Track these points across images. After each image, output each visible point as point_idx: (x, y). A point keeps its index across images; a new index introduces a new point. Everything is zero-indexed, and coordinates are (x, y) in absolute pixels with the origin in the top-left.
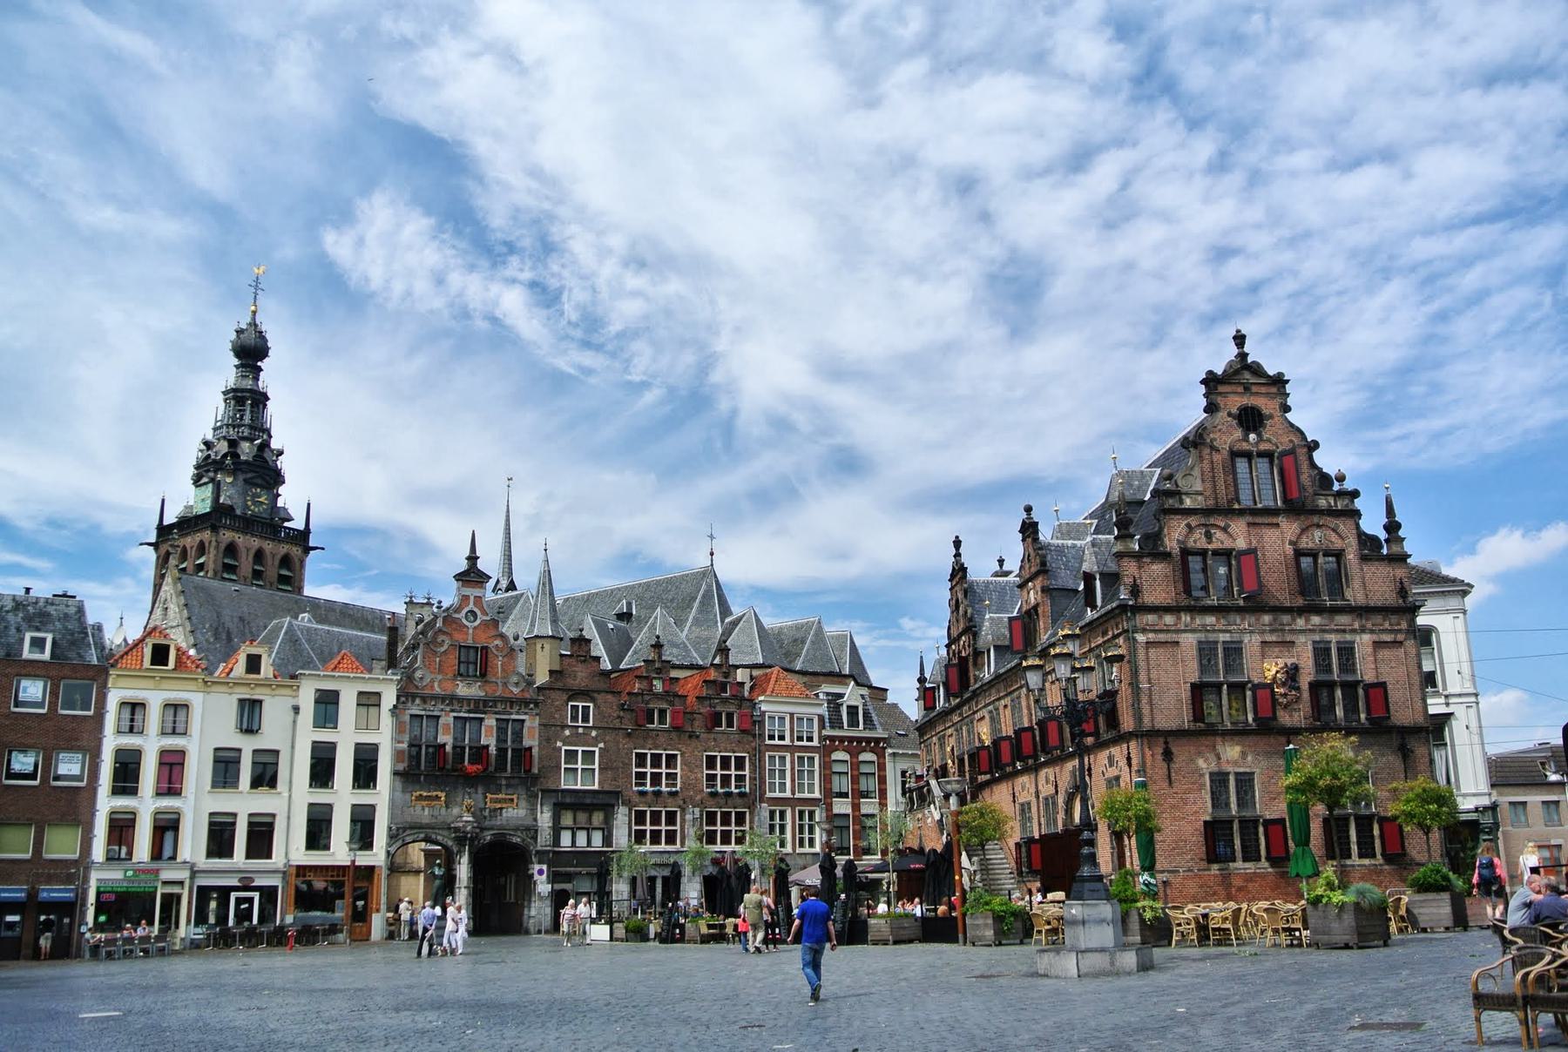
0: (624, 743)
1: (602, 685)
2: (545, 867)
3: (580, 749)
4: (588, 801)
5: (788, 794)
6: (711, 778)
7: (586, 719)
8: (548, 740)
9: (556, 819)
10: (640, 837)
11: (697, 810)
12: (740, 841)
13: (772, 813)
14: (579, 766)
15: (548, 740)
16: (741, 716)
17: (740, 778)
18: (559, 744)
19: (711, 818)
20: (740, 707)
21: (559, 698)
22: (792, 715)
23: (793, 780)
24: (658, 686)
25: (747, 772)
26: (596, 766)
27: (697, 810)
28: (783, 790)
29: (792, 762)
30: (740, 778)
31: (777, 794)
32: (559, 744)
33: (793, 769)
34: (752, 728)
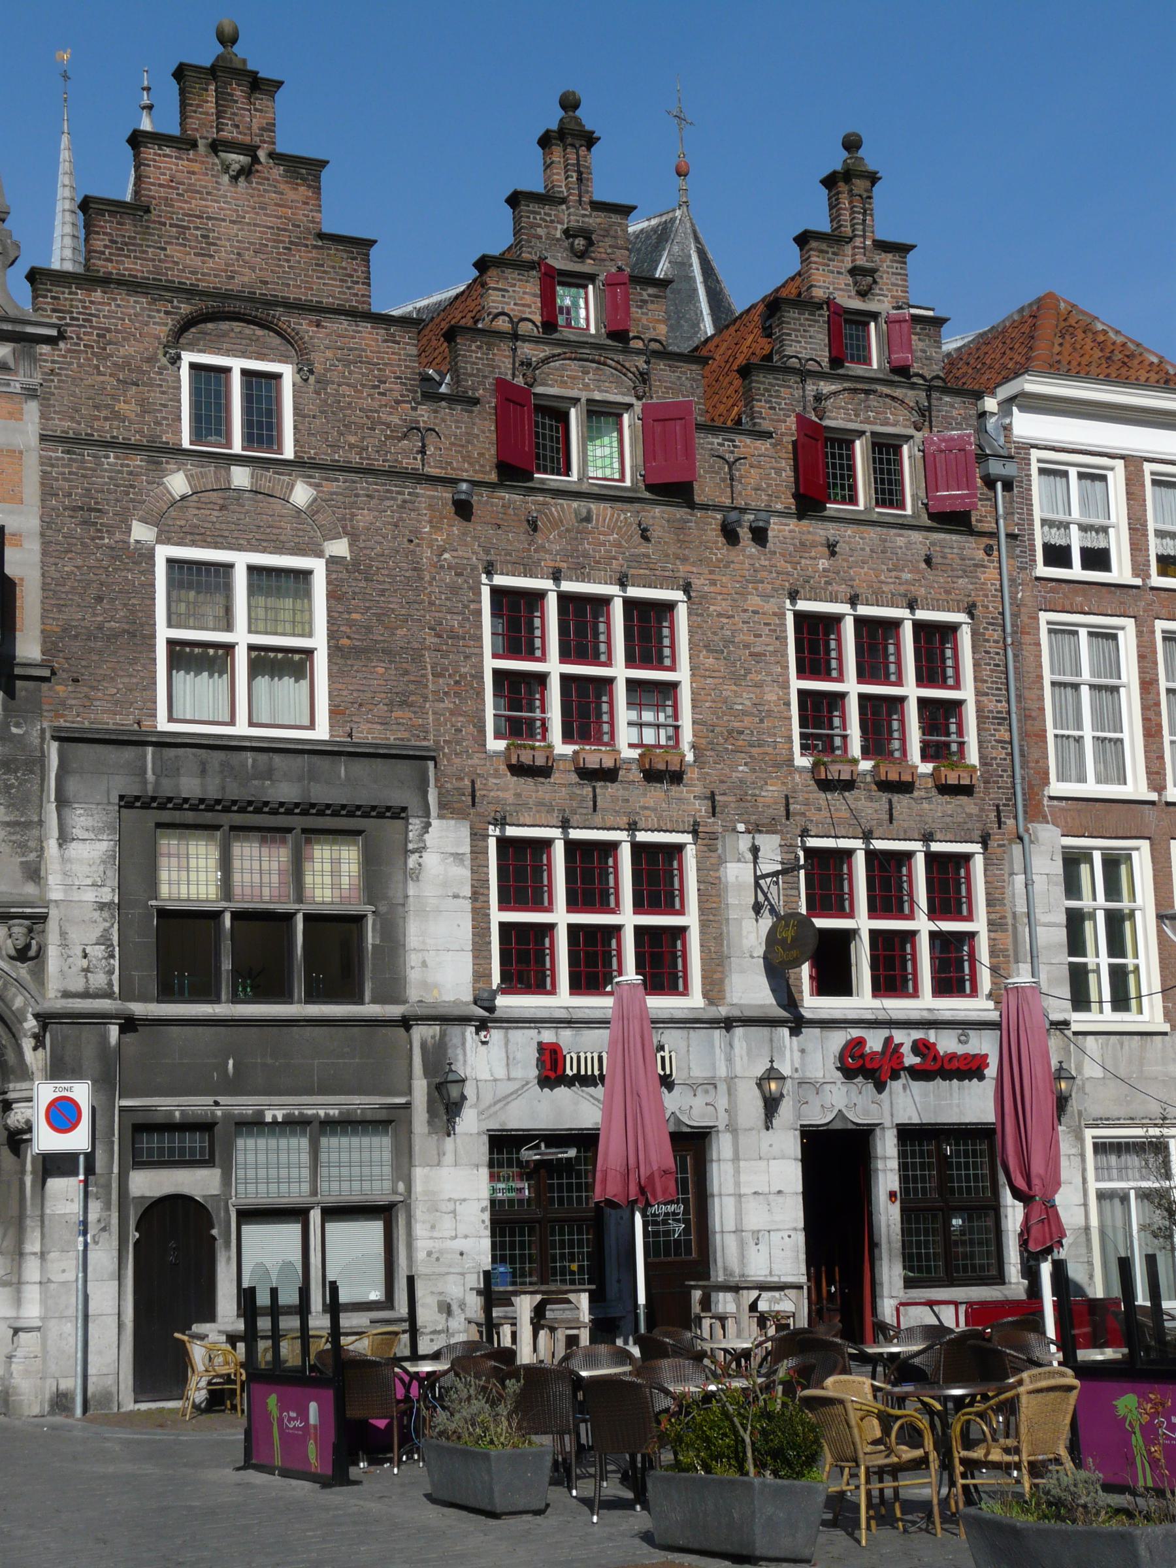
0: (441, 539)
1: (329, 291)
2: (81, 1092)
3: (241, 560)
4: (286, 792)
5: (1136, 787)
6: (819, 710)
7: (262, 427)
8: (87, 512)
9: (136, 867)
10: (524, 958)
11: (770, 845)
12: (952, 977)
13: (1073, 861)
14: (241, 637)
15: (87, 512)
16: (928, 461)
17: (940, 716)
18: (141, 532)
19: (826, 871)
20: (925, 415)
21: (142, 322)
22: (1134, 463)
23: (1152, 732)
24: (584, 311)
25: (967, 693)
26: (319, 642)
27: (770, 845)
28: (1115, 771)
29: (1146, 657)
30: (940, 716)
31: (1090, 788)
32: (141, 532)
33: (1148, 685)
34: (971, 499)
